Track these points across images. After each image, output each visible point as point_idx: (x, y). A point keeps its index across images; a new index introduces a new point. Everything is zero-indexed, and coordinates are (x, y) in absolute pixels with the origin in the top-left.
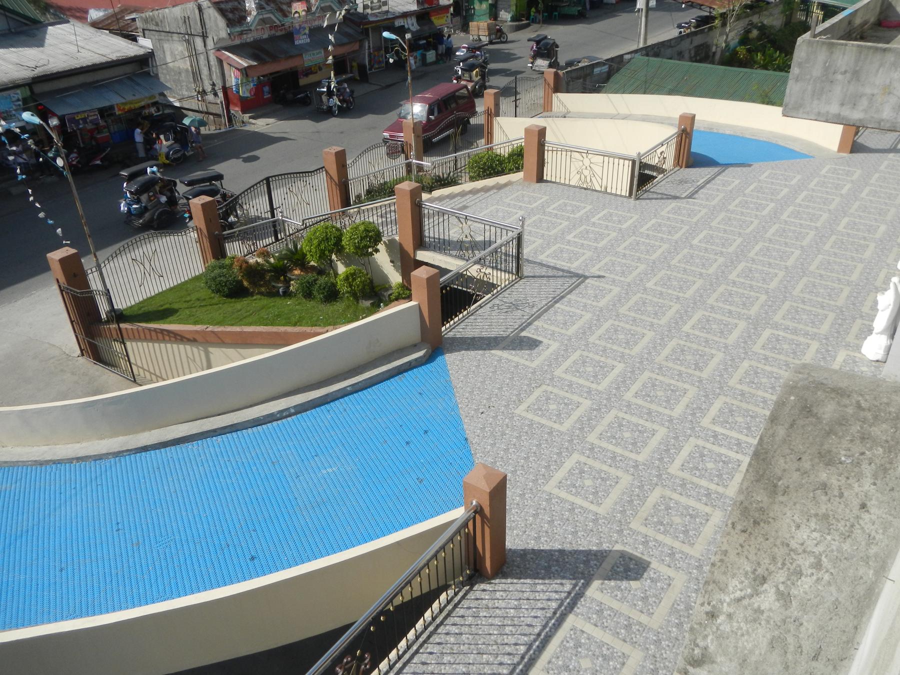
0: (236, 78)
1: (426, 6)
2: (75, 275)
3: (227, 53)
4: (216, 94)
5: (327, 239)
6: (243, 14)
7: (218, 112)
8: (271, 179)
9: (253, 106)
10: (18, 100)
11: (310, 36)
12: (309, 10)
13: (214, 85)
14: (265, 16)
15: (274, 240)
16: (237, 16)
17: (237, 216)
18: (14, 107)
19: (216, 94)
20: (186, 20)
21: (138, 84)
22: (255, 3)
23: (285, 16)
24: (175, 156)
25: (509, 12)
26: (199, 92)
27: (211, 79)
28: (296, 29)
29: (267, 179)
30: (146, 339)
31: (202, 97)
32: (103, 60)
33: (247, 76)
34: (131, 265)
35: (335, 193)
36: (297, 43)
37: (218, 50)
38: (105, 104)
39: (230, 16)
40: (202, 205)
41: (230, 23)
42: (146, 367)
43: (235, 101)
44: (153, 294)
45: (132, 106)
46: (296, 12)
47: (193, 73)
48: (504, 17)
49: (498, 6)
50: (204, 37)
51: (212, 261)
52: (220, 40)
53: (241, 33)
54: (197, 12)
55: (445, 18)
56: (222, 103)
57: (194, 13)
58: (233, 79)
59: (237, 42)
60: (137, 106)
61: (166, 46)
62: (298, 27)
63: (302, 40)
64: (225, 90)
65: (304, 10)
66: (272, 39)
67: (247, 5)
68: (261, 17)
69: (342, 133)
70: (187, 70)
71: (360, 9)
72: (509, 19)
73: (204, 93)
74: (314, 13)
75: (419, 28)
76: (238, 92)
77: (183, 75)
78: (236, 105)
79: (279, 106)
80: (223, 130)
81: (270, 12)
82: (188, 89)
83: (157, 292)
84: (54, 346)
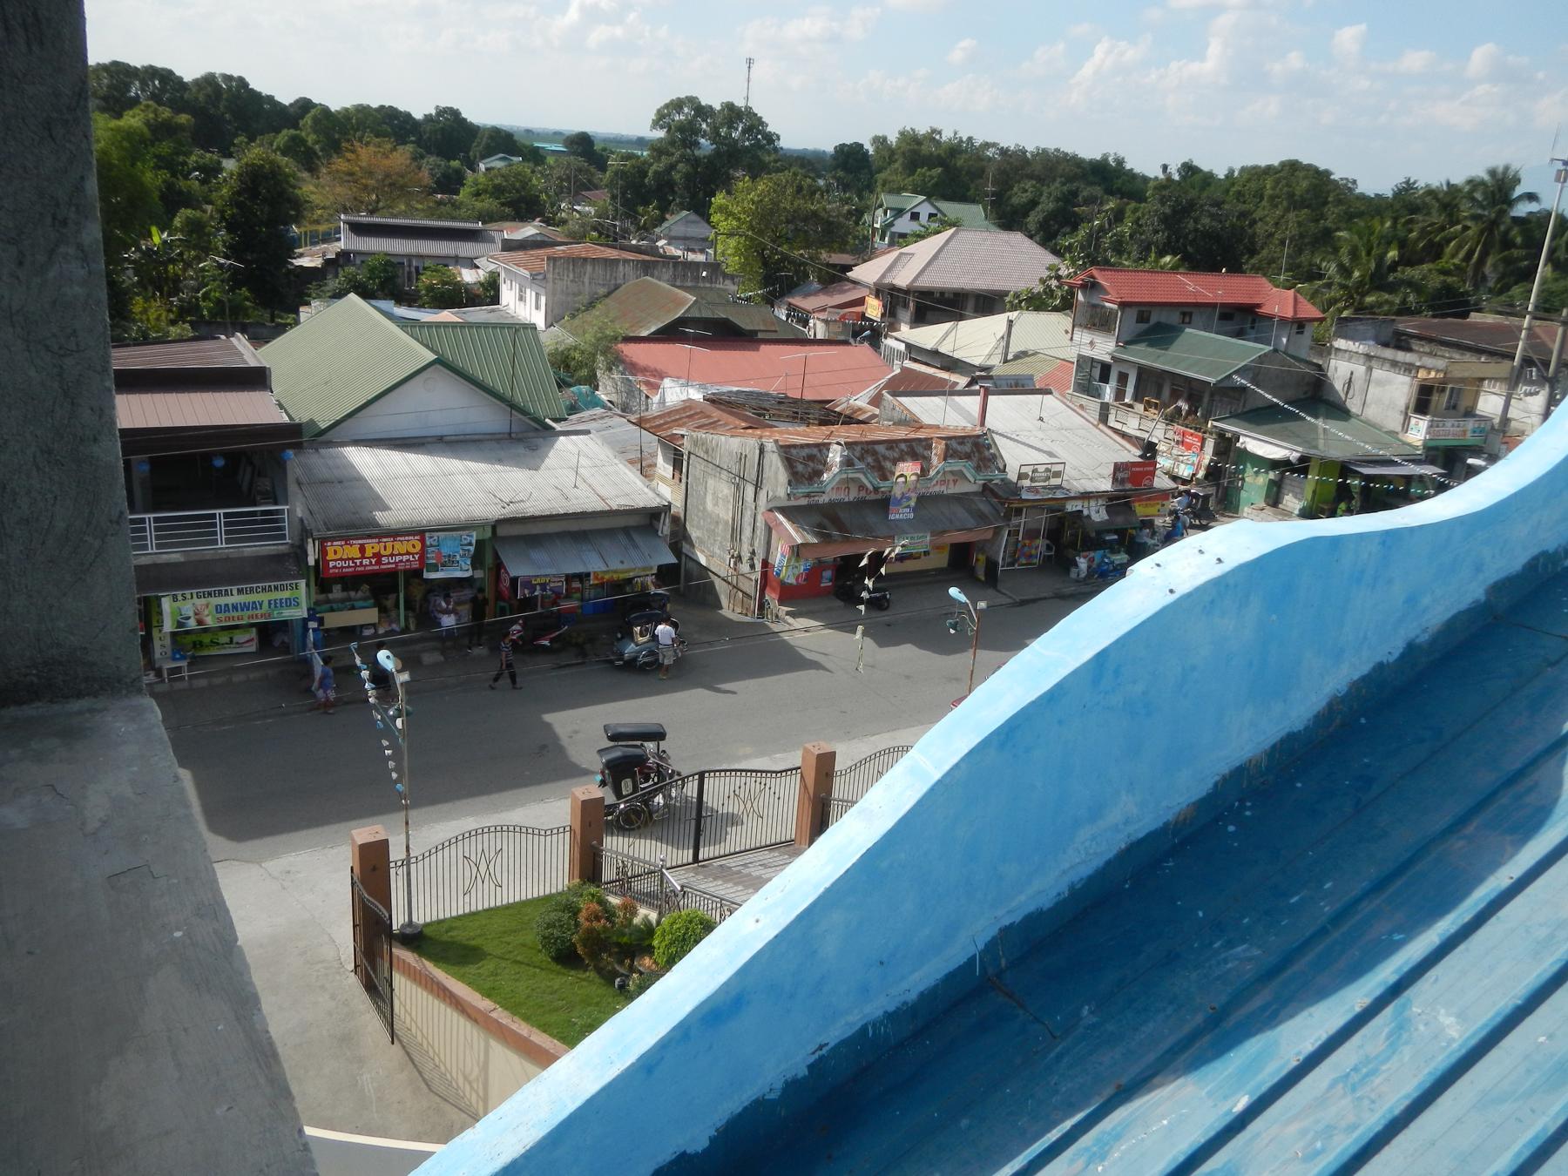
0: (782, 555)
1: (1128, 486)
2: (374, 869)
3: (781, 517)
4: (752, 566)
5: (684, 940)
6: (821, 467)
7: (748, 592)
8: (707, 775)
9: (798, 596)
10: (470, 544)
11: (915, 510)
12: (924, 472)
13: (753, 553)
14: (851, 476)
15: (690, 860)
16: (810, 470)
17: (667, 797)
18: (461, 552)
19: (752, 566)
20: (742, 458)
21: (636, 547)
22: (841, 456)
23: (884, 478)
24: (646, 660)
25: (1300, 500)
26: (733, 557)
27: (752, 545)
28: (895, 498)
29: (702, 775)
30: (426, 987)
31: (735, 564)
32: (599, 506)
33: (798, 555)
34: (460, 862)
35: (806, 812)
36: (891, 517)
37: (770, 510)
38: (579, 569)
39: (800, 468)
40: (583, 801)
41: (795, 478)
42: (419, 1025)
43: (775, 584)
44: (480, 908)
45: (615, 576)
46: (902, 475)
47: (733, 529)
48: (1289, 504)
49: (1284, 486)
50: (758, 486)
51: (577, 880)
52: (775, 498)
53: (808, 495)
54: (757, 452)
55: (1159, 507)
56: (757, 581)
57: (754, 453)
58: (779, 557)
59: (804, 502)
60: (622, 576)
61: (711, 482)
62: (899, 496)
63: (900, 514)
64: (765, 564)
65: (916, 474)
66: (859, 504)
67: (831, 455)
68: (844, 476)
69: (908, 677)
70: (727, 522)
71: (1012, 476)
72: (1297, 512)
73: (739, 558)
74: (931, 479)
75: (1106, 517)
76: (778, 574)
77: (720, 527)
78: (773, 590)
79: (842, 604)
80: (748, 619)
81: (860, 470)
82: (721, 547)
83: (486, 906)
84: (334, 941)
